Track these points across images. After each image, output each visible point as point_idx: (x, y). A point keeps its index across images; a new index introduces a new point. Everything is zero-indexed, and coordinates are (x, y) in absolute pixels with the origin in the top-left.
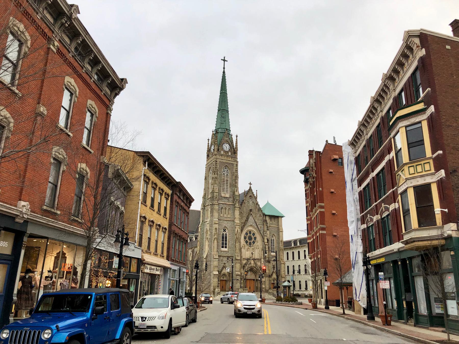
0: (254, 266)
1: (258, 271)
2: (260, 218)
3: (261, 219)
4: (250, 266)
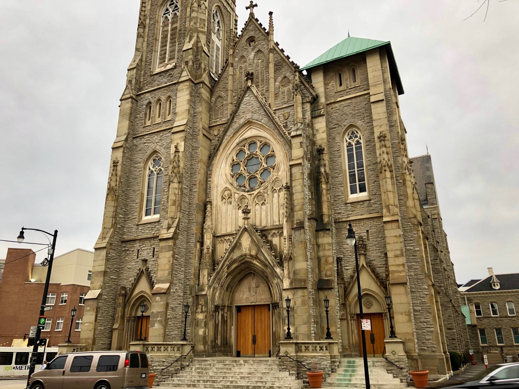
0: (253, 253)
1: (268, 271)
2: (286, 89)
3: (289, 91)
4: (236, 255)
